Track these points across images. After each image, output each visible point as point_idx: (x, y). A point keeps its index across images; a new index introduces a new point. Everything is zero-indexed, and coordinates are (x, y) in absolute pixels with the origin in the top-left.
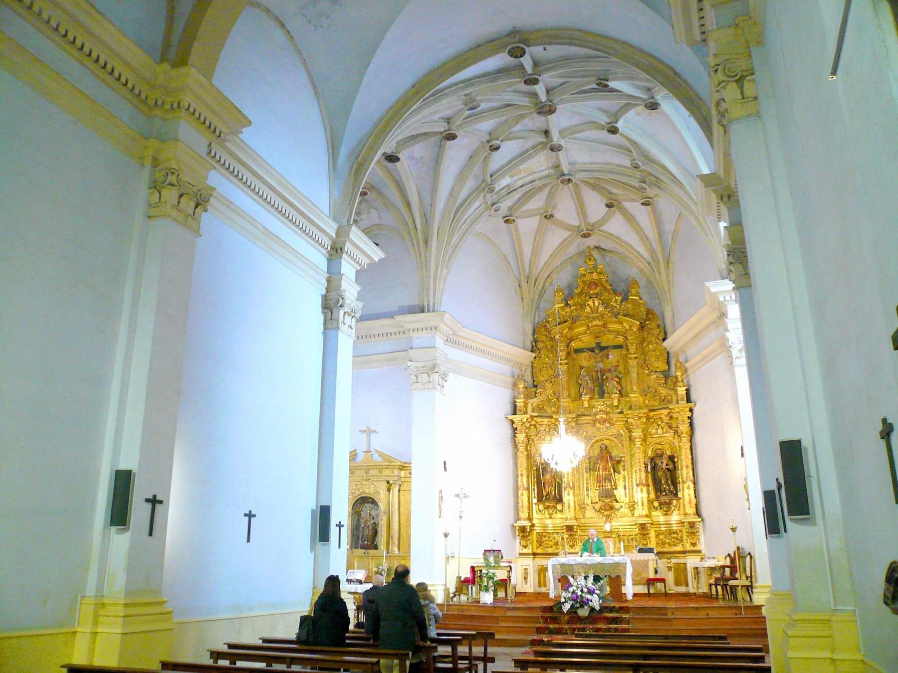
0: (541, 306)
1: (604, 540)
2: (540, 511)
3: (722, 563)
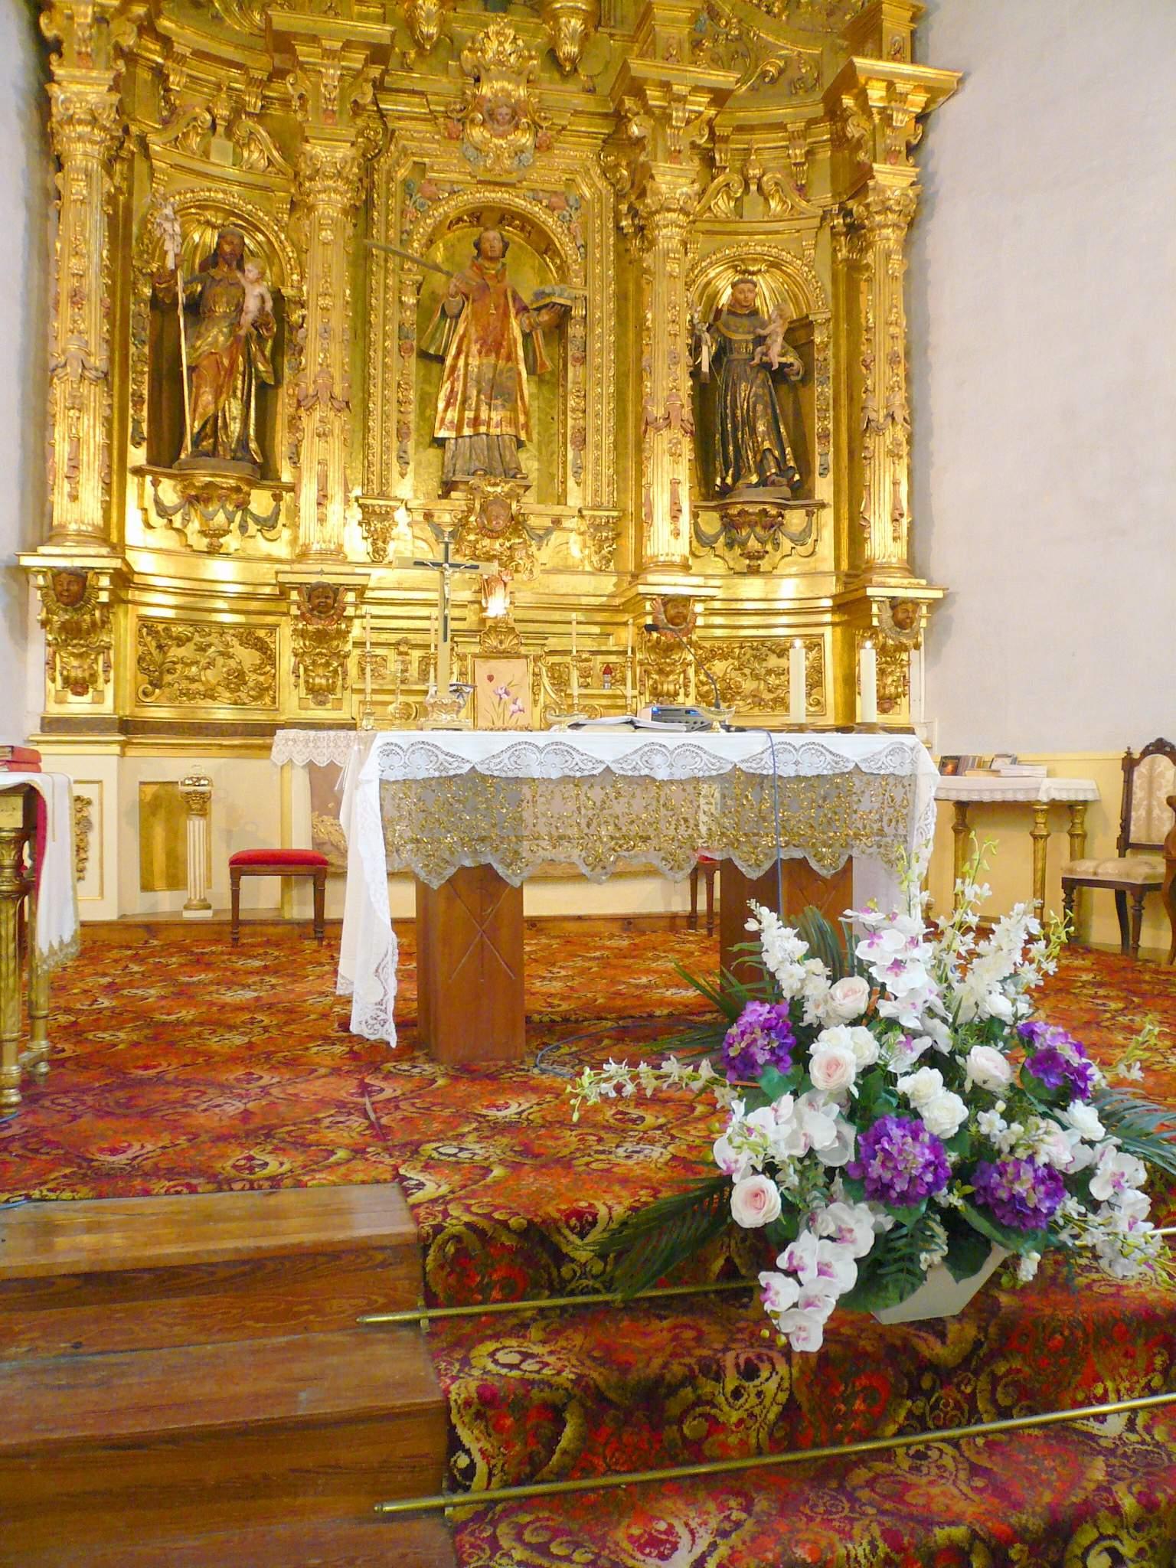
1: (483, 668)
2: (163, 511)
3: (1078, 774)
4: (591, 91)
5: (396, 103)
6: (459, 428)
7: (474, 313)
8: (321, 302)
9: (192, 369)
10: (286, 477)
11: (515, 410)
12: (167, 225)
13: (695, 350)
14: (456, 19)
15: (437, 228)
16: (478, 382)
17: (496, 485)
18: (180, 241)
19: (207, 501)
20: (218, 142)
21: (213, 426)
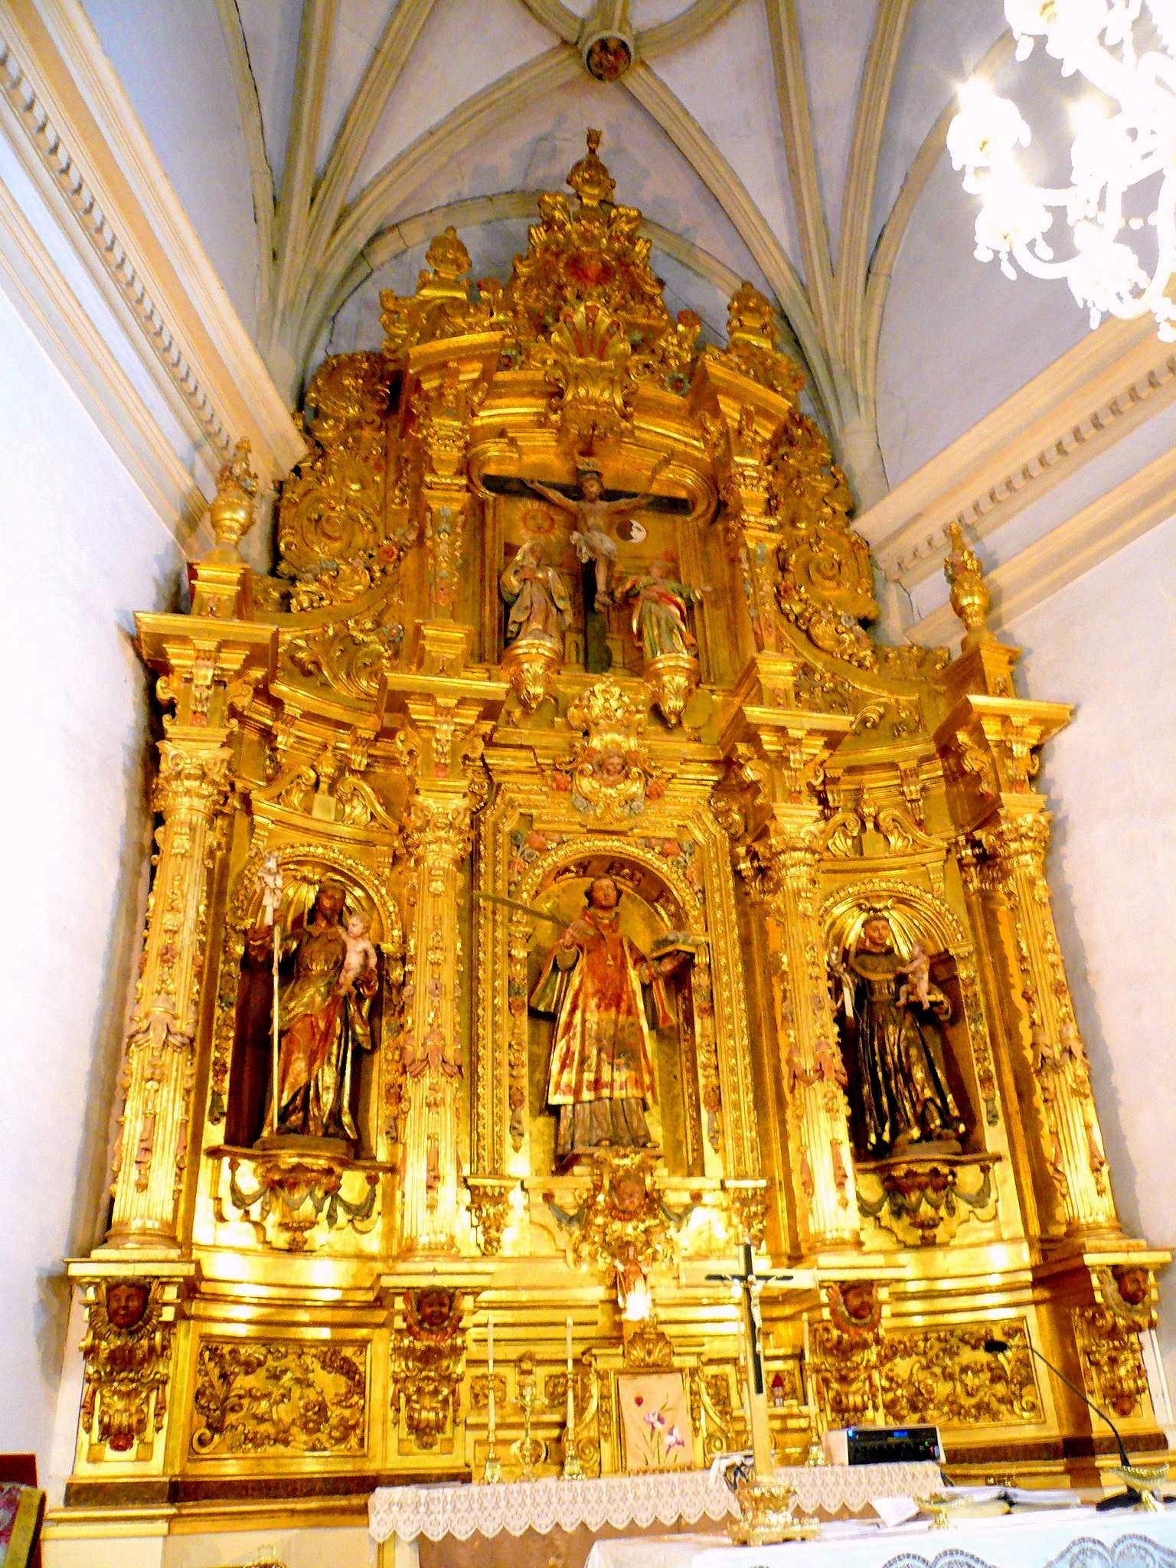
0: (349, 314)
1: (629, 1389)
4: (698, 740)
5: (503, 758)
6: (577, 1092)
7: (590, 965)
8: (432, 956)
9: (282, 1033)
10: (382, 1154)
11: (638, 1069)
12: (269, 880)
13: (836, 991)
14: (559, 682)
15: (546, 876)
16: (599, 1040)
17: (625, 1156)
18: (278, 895)
19: (294, 1186)
20: (321, 797)
21: (305, 1098)
